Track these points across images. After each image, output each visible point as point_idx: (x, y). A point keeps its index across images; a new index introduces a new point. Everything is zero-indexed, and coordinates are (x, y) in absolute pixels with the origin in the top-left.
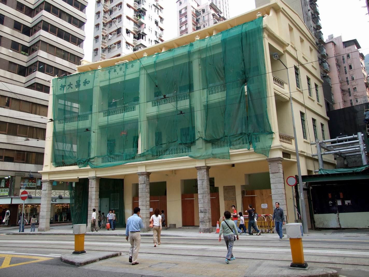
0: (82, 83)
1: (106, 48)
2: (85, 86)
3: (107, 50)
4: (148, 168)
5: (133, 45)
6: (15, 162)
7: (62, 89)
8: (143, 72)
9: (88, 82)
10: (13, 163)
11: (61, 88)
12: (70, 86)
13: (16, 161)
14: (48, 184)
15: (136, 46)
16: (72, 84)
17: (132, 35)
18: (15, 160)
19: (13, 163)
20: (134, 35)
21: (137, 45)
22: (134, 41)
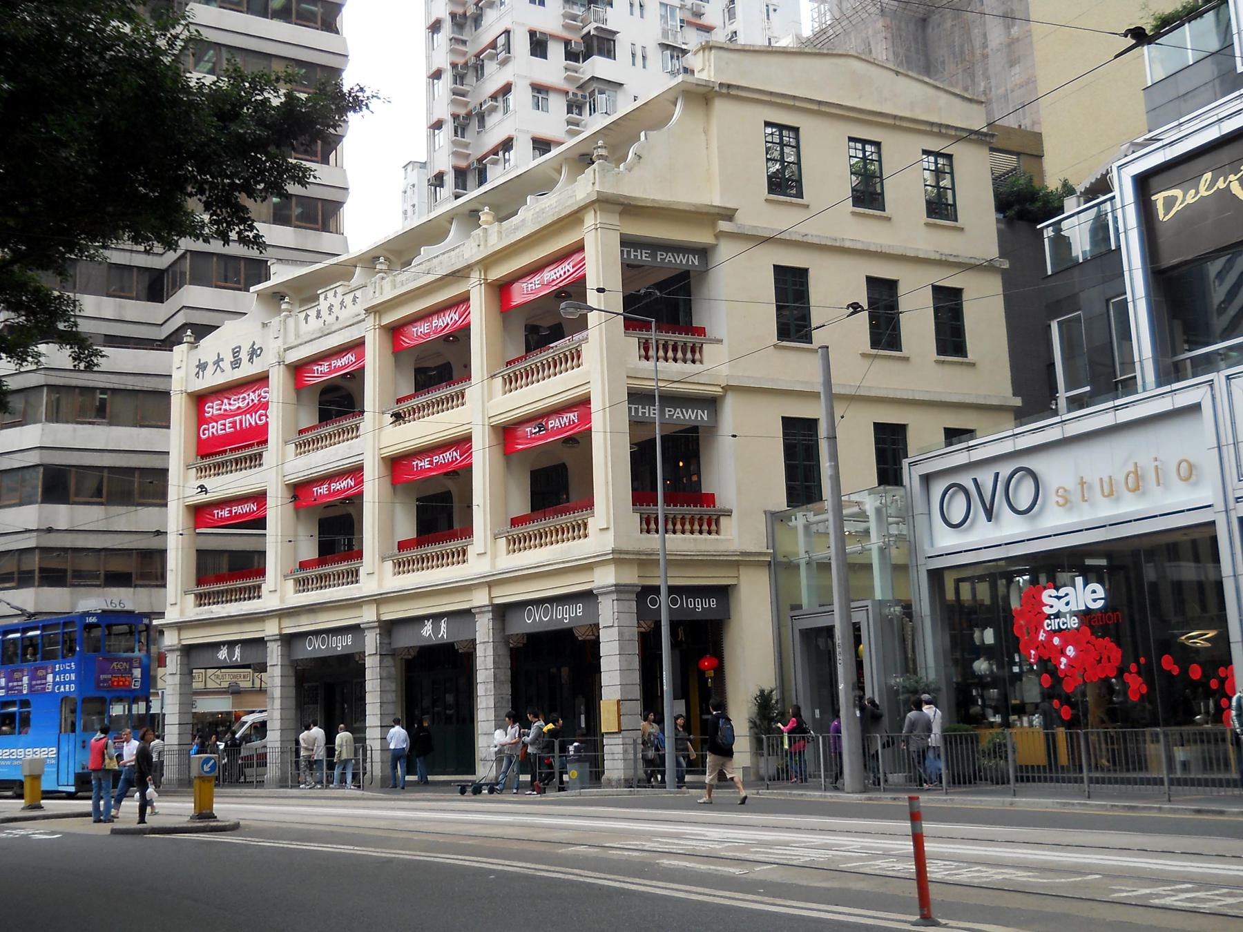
0: (244, 355)
1: (469, 116)
2: (252, 363)
3: (474, 123)
4: (383, 609)
5: (566, 86)
6: (136, 586)
7: (201, 373)
8: (371, 321)
9: (259, 352)
10: (132, 589)
11: (198, 373)
12: (219, 366)
13: (139, 582)
14: (179, 658)
15: (580, 87)
16: (222, 360)
17: (556, 51)
18: (137, 579)
19: (131, 590)
20: (567, 43)
21: (582, 81)
22: (566, 69)
